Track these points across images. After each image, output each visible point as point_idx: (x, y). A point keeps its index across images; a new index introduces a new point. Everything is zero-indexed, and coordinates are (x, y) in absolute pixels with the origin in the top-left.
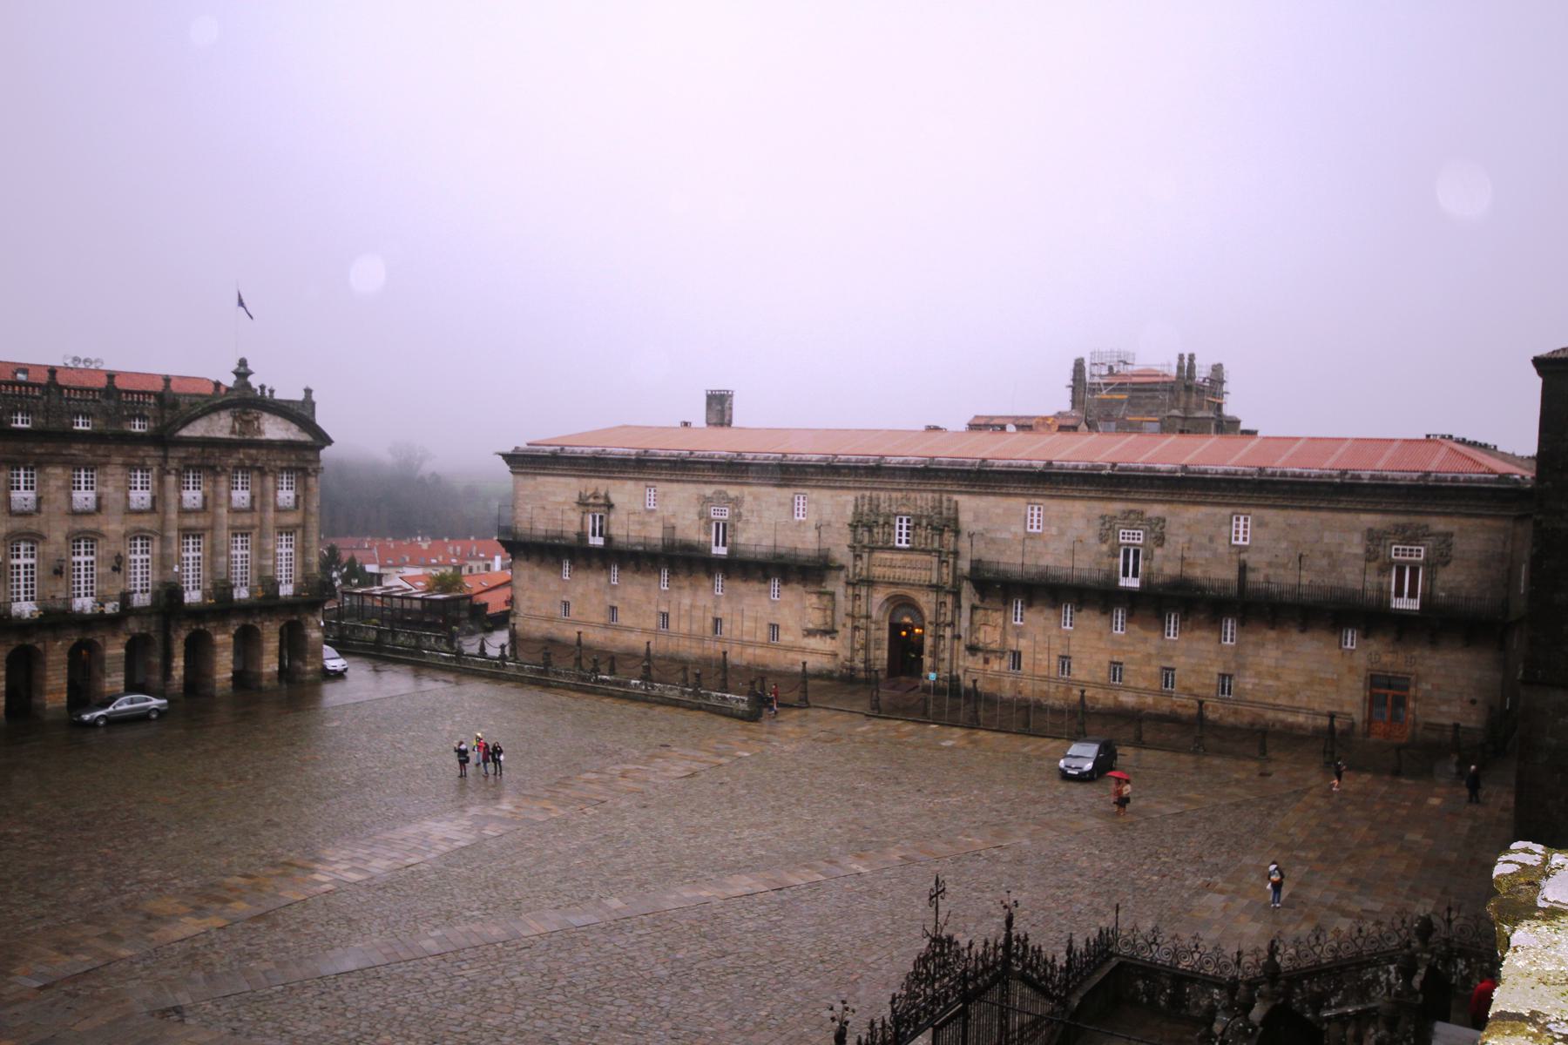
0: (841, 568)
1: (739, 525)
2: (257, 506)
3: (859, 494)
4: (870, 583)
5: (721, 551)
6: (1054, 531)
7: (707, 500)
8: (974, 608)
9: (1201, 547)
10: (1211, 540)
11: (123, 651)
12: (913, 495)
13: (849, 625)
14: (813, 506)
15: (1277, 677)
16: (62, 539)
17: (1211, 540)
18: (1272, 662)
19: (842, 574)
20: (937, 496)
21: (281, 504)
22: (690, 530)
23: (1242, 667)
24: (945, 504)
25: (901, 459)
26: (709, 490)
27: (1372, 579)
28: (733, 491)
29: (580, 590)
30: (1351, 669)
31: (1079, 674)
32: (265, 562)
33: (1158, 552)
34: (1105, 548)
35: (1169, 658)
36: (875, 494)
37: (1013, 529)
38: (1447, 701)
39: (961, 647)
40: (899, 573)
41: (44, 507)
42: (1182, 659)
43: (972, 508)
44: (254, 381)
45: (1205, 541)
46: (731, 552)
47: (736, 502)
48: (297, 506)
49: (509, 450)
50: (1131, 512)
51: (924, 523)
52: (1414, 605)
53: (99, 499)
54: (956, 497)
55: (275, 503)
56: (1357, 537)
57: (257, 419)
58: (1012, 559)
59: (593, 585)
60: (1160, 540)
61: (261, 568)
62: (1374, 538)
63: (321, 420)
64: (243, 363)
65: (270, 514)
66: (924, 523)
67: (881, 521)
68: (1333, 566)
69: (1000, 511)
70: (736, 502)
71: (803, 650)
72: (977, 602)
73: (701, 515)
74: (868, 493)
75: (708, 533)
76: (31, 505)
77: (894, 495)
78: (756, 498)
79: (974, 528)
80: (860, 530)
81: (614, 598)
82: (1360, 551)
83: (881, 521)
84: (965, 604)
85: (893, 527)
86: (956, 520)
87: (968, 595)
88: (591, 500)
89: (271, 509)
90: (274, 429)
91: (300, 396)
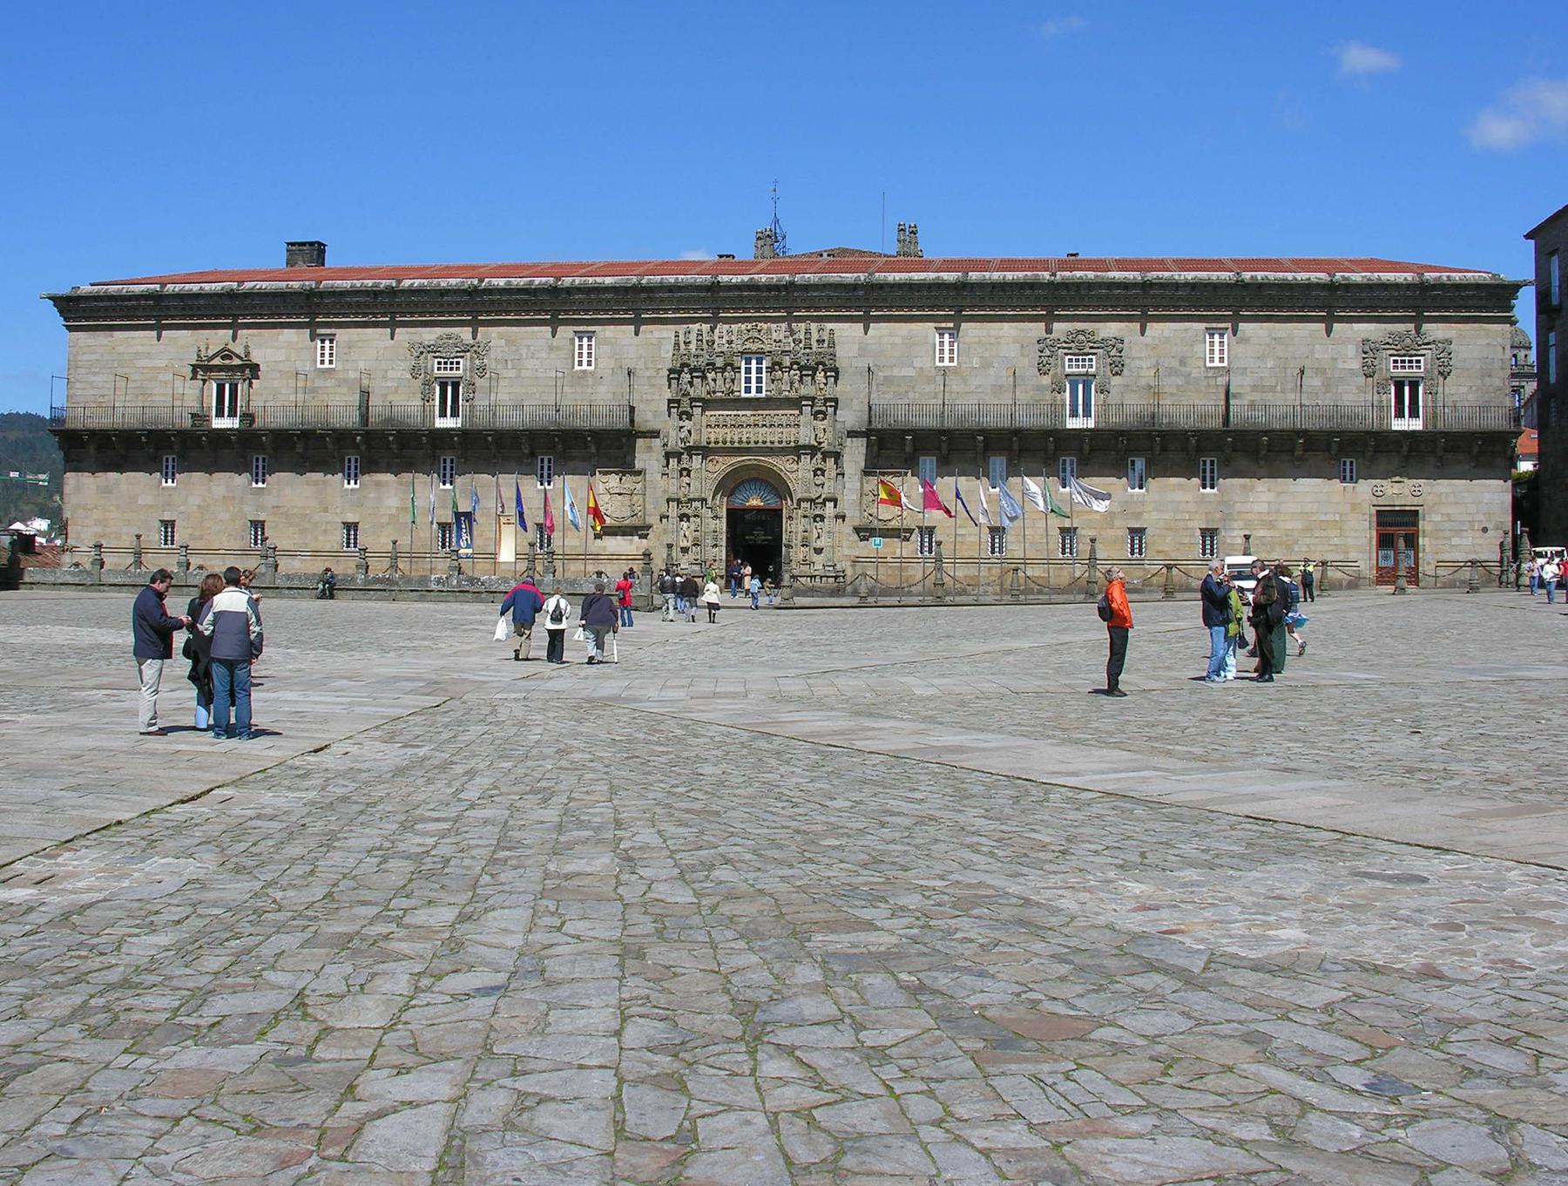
0: (655, 434)
3: (682, 328)
4: (706, 451)
6: (976, 362)
9: (1172, 372)
10: (1183, 362)
13: (673, 511)
14: (606, 349)
15: (1271, 525)
17: (1183, 362)
18: (1264, 508)
19: (657, 442)
23: (1227, 518)
24: (815, 336)
26: (430, 335)
27: (1370, 396)
29: (195, 501)
30: (1354, 507)
31: (1014, 547)
33: (1116, 380)
34: (1046, 380)
35: (1138, 515)
37: (917, 363)
38: (1458, 532)
39: (847, 528)
40: (747, 435)
42: (1154, 516)
45: (1175, 363)
49: (65, 291)
50: (1079, 332)
51: (787, 361)
52: (1417, 425)
54: (829, 326)
56: (1351, 351)
58: (918, 404)
60: (1117, 368)
62: (1369, 350)
66: (787, 361)
67: (720, 362)
68: (1327, 386)
71: (596, 557)
73: (415, 372)
75: (427, 399)
80: (686, 377)
81: (260, 508)
82: (1356, 365)
83: (720, 362)
85: (737, 369)
87: (855, 454)
88: (217, 361)
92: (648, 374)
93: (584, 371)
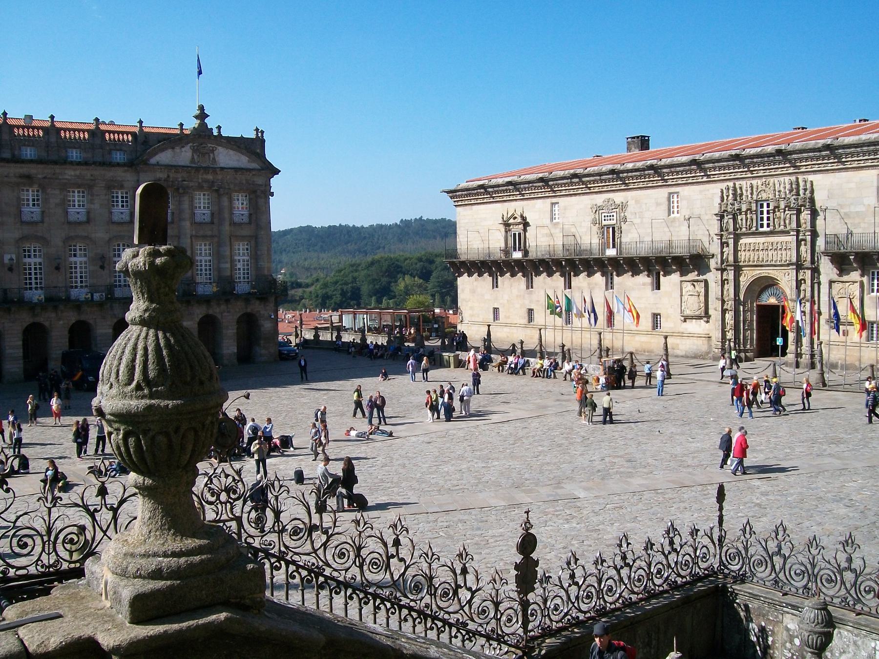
1: (624, 226)
2: (216, 221)
3: (723, 185)
5: (611, 252)
7: (598, 209)
8: (831, 282)
11: (111, 331)
12: (772, 180)
16: (61, 244)
20: (793, 178)
21: (236, 220)
22: (590, 240)
24: (801, 184)
25: (759, 149)
26: (599, 199)
28: (618, 197)
32: (223, 266)
36: (738, 183)
37: (866, 201)
41: (46, 219)
43: (827, 185)
44: (211, 123)
46: (620, 251)
47: (623, 207)
48: (250, 223)
53: (88, 213)
54: (810, 177)
55: (231, 219)
57: (213, 151)
59: (515, 291)
61: (219, 270)
63: (272, 155)
64: (201, 108)
65: (227, 228)
69: (852, 185)
70: (623, 207)
72: (835, 277)
74: (731, 184)
76: (37, 217)
77: (754, 182)
78: (637, 202)
79: (830, 204)
84: (824, 279)
86: (812, 200)
89: (227, 223)
90: (226, 158)
91: (252, 135)
92: (707, 217)
93: (674, 218)
